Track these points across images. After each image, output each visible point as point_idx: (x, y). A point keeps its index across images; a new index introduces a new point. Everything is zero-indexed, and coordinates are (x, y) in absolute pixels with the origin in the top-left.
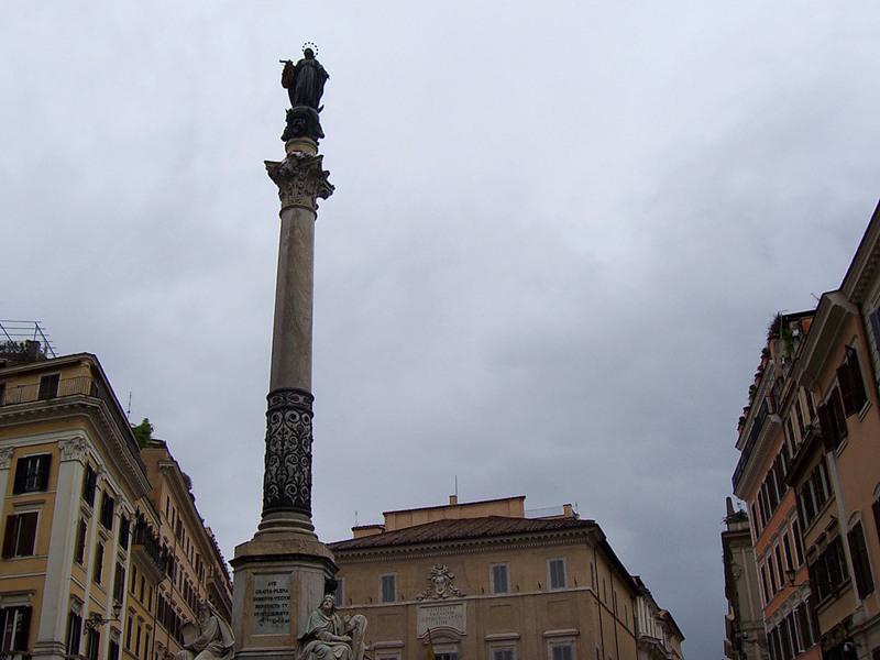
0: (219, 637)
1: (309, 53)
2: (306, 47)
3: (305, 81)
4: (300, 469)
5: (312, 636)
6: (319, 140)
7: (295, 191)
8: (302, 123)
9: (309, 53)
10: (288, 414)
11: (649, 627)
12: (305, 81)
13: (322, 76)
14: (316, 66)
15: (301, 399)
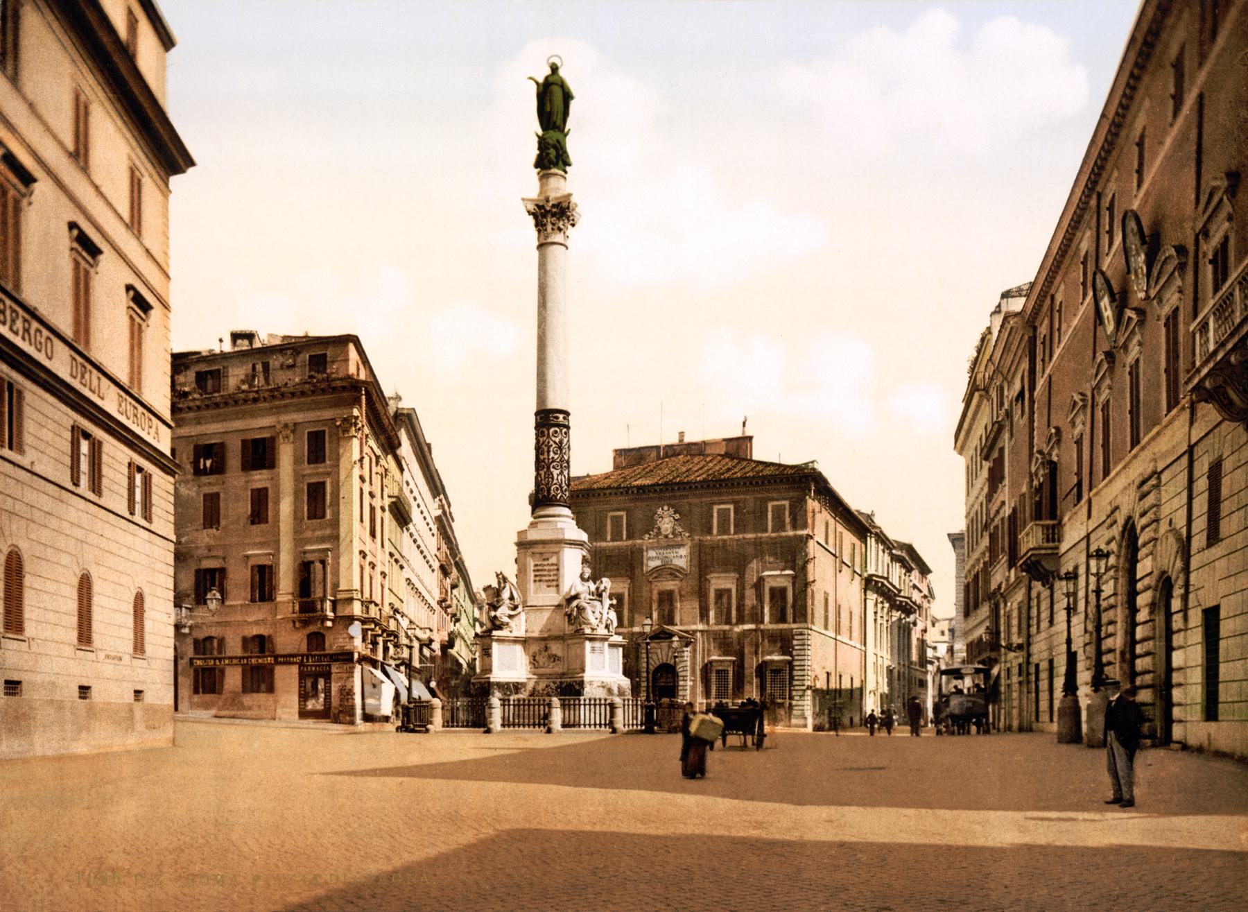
0: (512, 598)
1: (554, 69)
2: (552, 61)
3: (553, 101)
4: (561, 473)
5: (576, 597)
6: (568, 168)
7: (549, 227)
8: (553, 152)
9: (554, 69)
10: (552, 430)
11: (878, 562)
12: (553, 101)
13: (567, 97)
14: (563, 85)
15: (561, 416)
